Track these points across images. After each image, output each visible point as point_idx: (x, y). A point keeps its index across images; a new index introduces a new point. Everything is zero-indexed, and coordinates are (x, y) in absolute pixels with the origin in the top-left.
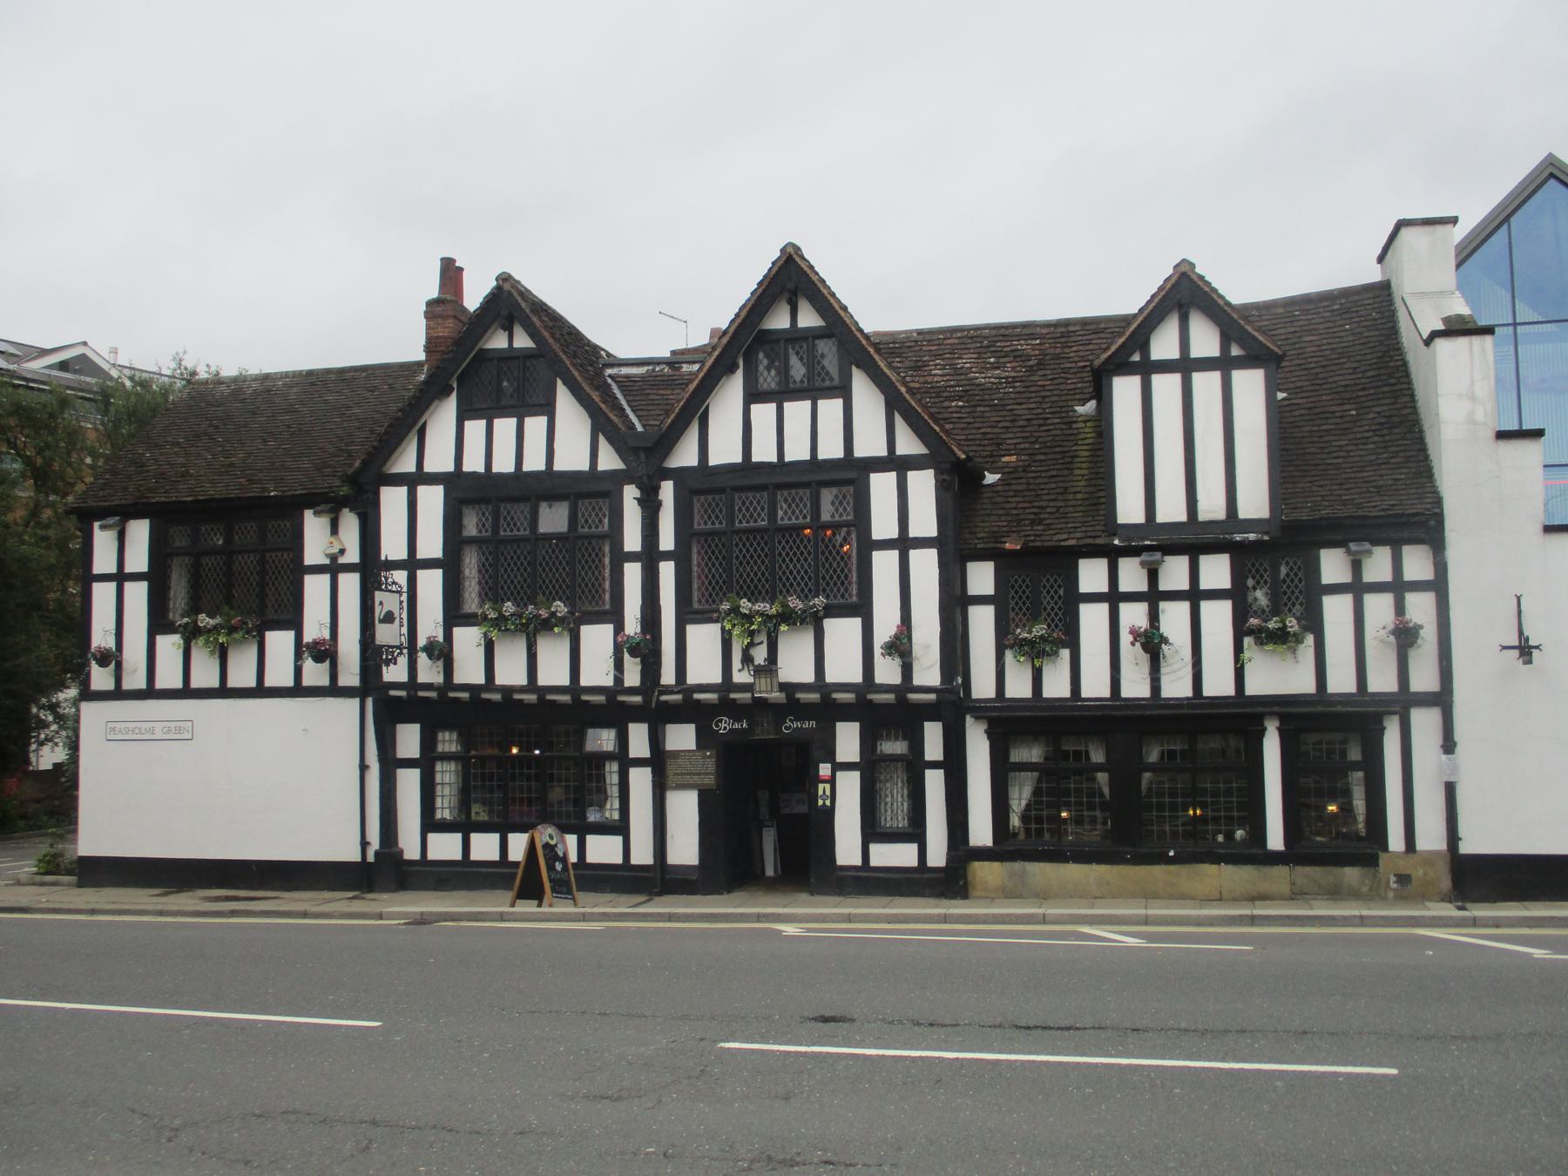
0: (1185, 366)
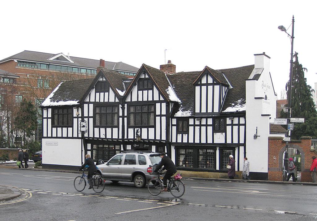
0: (207, 85)
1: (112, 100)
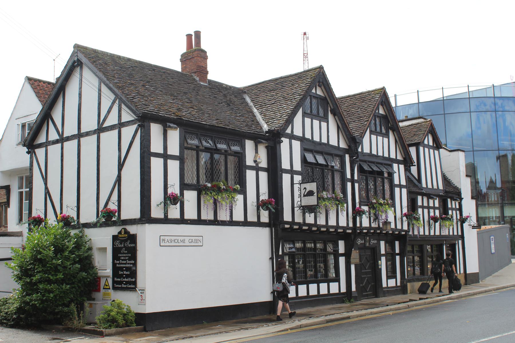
1: (333, 142)
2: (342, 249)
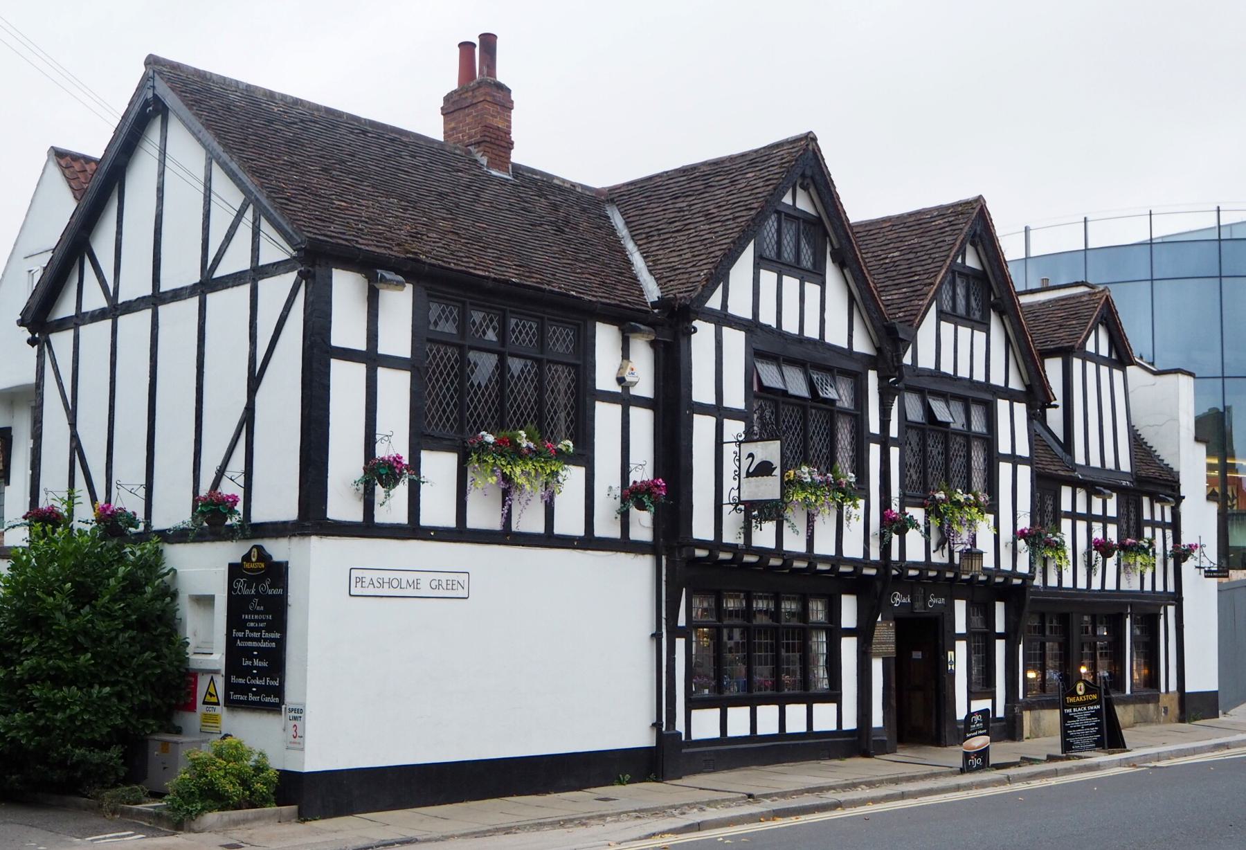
1: (836, 336)
2: (849, 614)
